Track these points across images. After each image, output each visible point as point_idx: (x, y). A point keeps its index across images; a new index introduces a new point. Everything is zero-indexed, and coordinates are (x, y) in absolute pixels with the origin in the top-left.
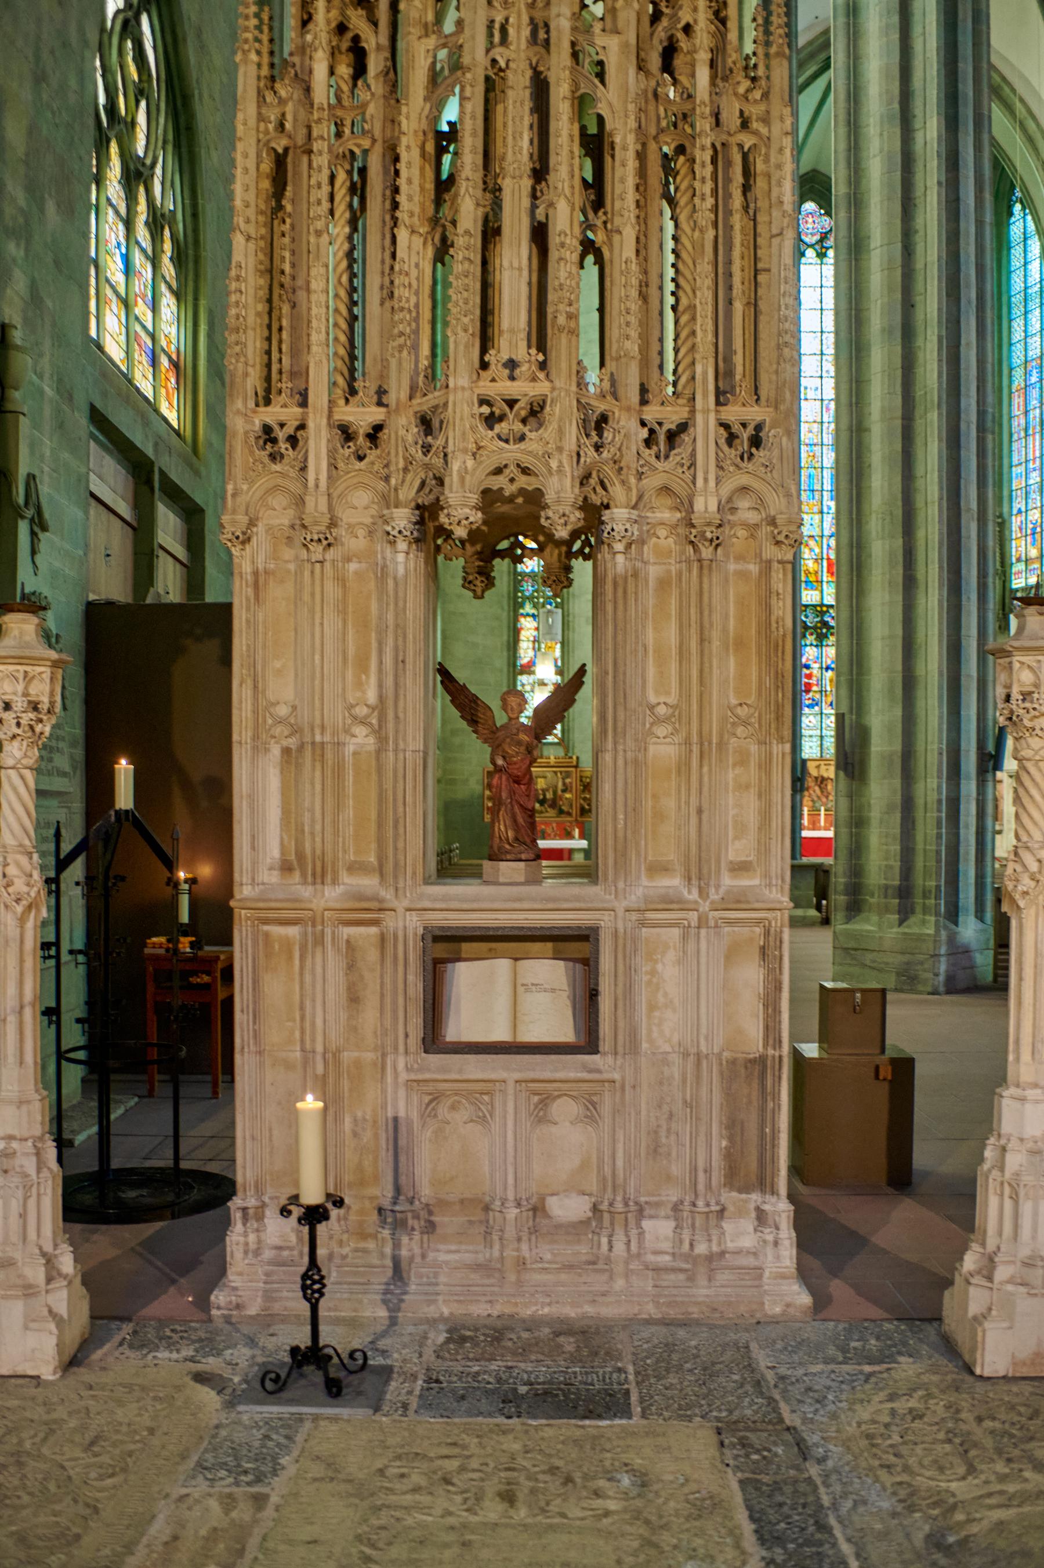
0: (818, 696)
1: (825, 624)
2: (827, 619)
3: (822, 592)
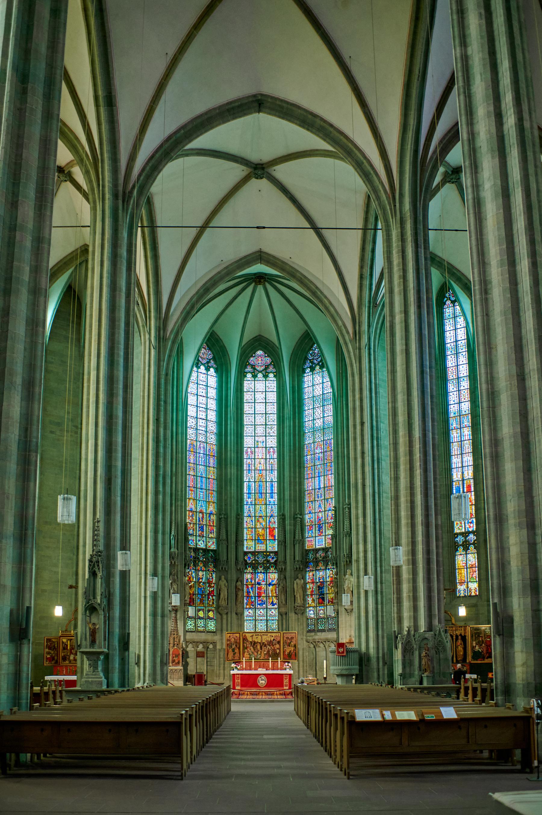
0: (265, 599)
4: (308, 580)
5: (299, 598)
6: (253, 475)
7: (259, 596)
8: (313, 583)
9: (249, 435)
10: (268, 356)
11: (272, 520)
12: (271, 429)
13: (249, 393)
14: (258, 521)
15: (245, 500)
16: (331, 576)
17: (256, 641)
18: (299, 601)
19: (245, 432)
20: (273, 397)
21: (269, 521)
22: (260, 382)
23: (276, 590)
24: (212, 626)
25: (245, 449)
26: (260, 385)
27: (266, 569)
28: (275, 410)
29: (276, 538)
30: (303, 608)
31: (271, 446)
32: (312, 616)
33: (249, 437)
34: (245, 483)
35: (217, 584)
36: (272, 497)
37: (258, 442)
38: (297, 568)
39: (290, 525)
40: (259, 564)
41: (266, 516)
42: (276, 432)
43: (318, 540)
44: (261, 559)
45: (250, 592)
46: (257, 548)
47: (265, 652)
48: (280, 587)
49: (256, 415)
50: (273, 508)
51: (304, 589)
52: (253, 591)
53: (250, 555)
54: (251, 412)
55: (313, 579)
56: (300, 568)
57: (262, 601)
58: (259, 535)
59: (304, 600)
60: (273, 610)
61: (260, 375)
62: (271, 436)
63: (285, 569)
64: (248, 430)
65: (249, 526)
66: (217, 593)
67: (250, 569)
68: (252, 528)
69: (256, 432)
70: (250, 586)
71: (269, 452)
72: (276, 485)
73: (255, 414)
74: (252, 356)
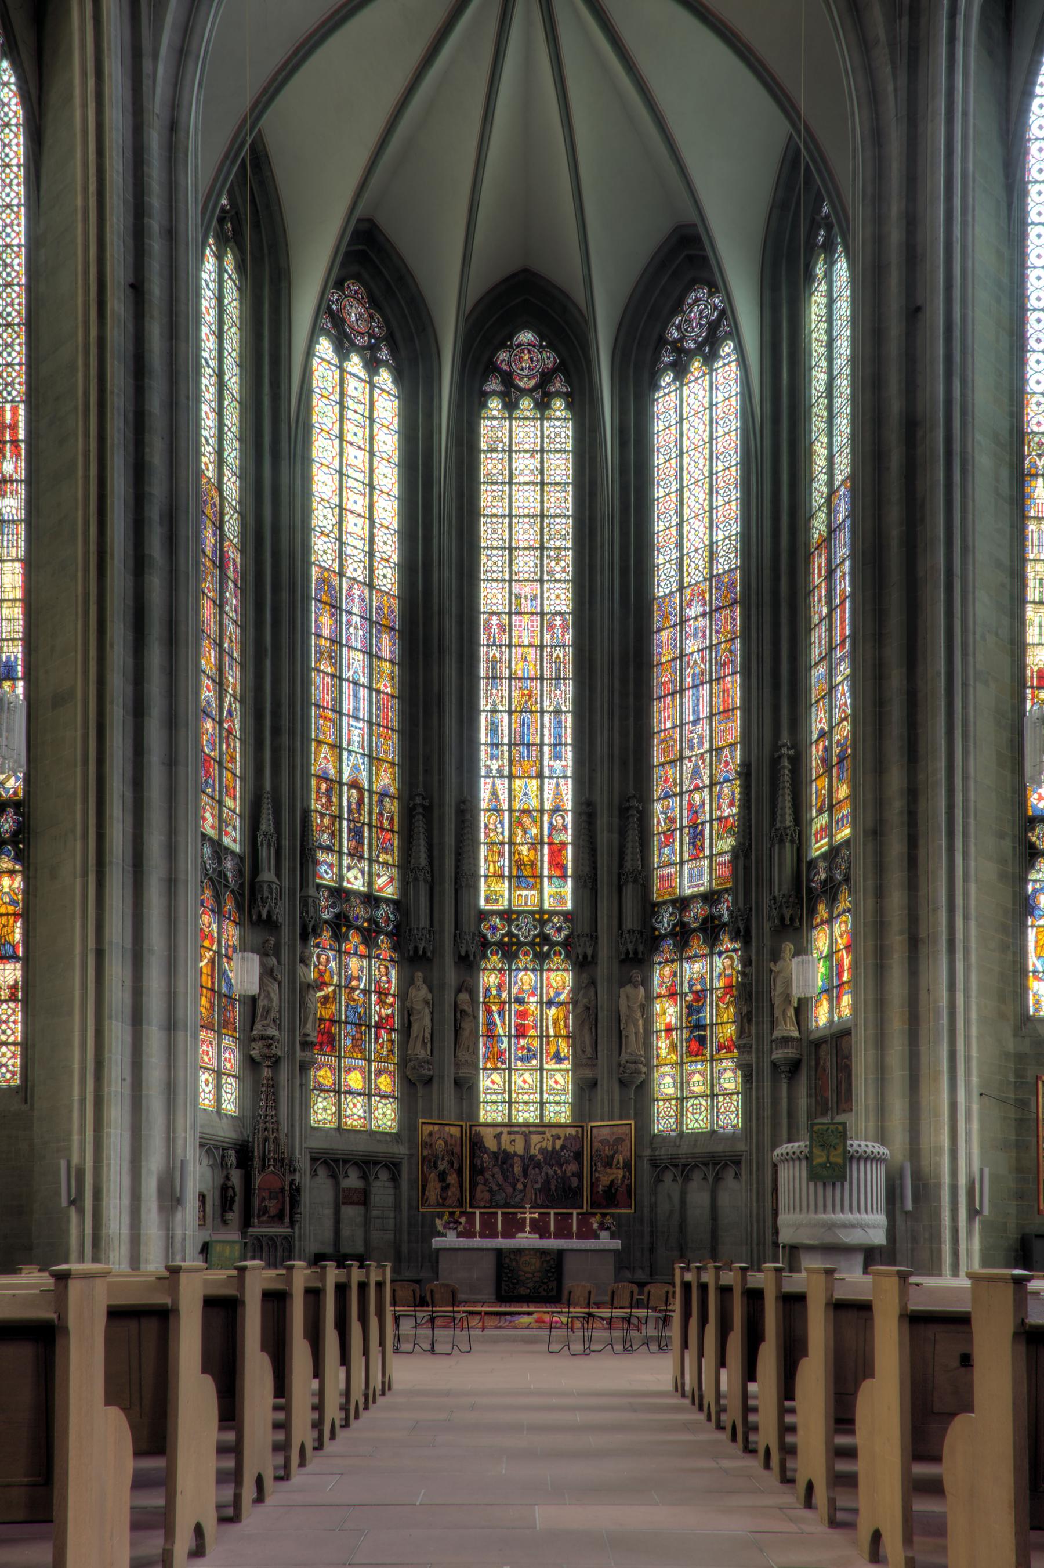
0: (536, 1043)
1: (546, 939)
2: (548, 929)
3: (541, 892)
6: (506, 694)
7: (521, 1032)
8: (672, 995)
9: (495, 575)
10: (551, 346)
11: (558, 821)
12: (558, 559)
13: (494, 455)
14: (520, 823)
15: (482, 763)
17: (511, 1149)
19: (482, 569)
20: (561, 467)
21: (551, 823)
22: (527, 423)
23: (566, 1018)
24: (386, 1116)
25: (483, 617)
26: (526, 432)
27: (541, 958)
28: (570, 505)
29: (570, 872)
30: (644, 1069)
31: (558, 608)
32: (670, 1091)
33: (495, 584)
34: (483, 716)
35: (403, 995)
36: (557, 757)
37: (518, 597)
38: (628, 953)
39: (610, 831)
40: (520, 945)
41: (542, 811)
42: (570, 569)
43: (688, 872)
44: (525, 931)
45: (495, 1024)
46: (515, 902)
47: (538, 1186)
48: (579, 1010)
49: (514, 520)
50: (562, 788)
52: (503, 1023)
53: (497, 921)
54: (500, 512)
56: (636, 952)
57: (529, 1050)
58: (520, 864)
59: (648, 1046)
60: (558, 1077)
61: (526, 403)
62: (559, 581)
63: (594, 956)
64: (491, 563)
65: (494, 838)
66: (402, 1024)
67: (495, 960)
68: (502, 843)
69: (515, 568)
70: (494, 1008)
71: (551, 627)
72: (568, 720)
73: (510, 516)
74: (502, 345)
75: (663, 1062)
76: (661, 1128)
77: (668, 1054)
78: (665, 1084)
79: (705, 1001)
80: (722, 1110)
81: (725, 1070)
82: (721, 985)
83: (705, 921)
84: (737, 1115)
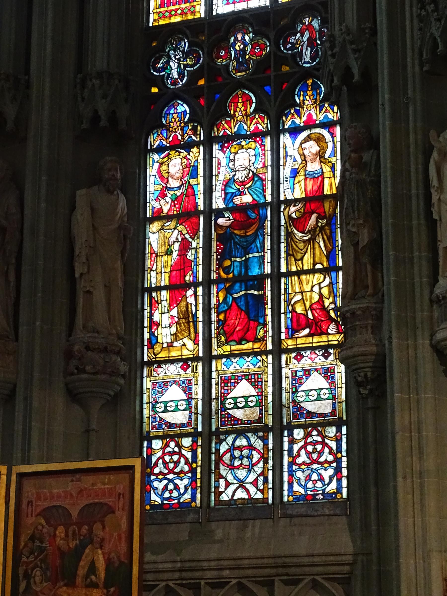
4: (152, 204)
5: (99, 295)
16: (313, 167)
18: (100, 317)
30: (123, 368)
32: (180, 418)
38: (96, 118)
51: (135, 256)
55: (191, 193)
56: (113, 118)
75: (163, 355)
76: (155, 498)
77: (176, 337)
78: (169, 397)
79: (262, 227)
80: (303, 458)
81: (308, 373)
82: (299, 194)
83: (263, 64)
84: (338, 470)
